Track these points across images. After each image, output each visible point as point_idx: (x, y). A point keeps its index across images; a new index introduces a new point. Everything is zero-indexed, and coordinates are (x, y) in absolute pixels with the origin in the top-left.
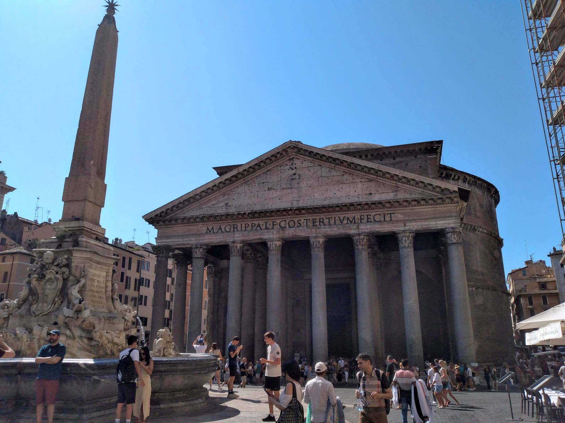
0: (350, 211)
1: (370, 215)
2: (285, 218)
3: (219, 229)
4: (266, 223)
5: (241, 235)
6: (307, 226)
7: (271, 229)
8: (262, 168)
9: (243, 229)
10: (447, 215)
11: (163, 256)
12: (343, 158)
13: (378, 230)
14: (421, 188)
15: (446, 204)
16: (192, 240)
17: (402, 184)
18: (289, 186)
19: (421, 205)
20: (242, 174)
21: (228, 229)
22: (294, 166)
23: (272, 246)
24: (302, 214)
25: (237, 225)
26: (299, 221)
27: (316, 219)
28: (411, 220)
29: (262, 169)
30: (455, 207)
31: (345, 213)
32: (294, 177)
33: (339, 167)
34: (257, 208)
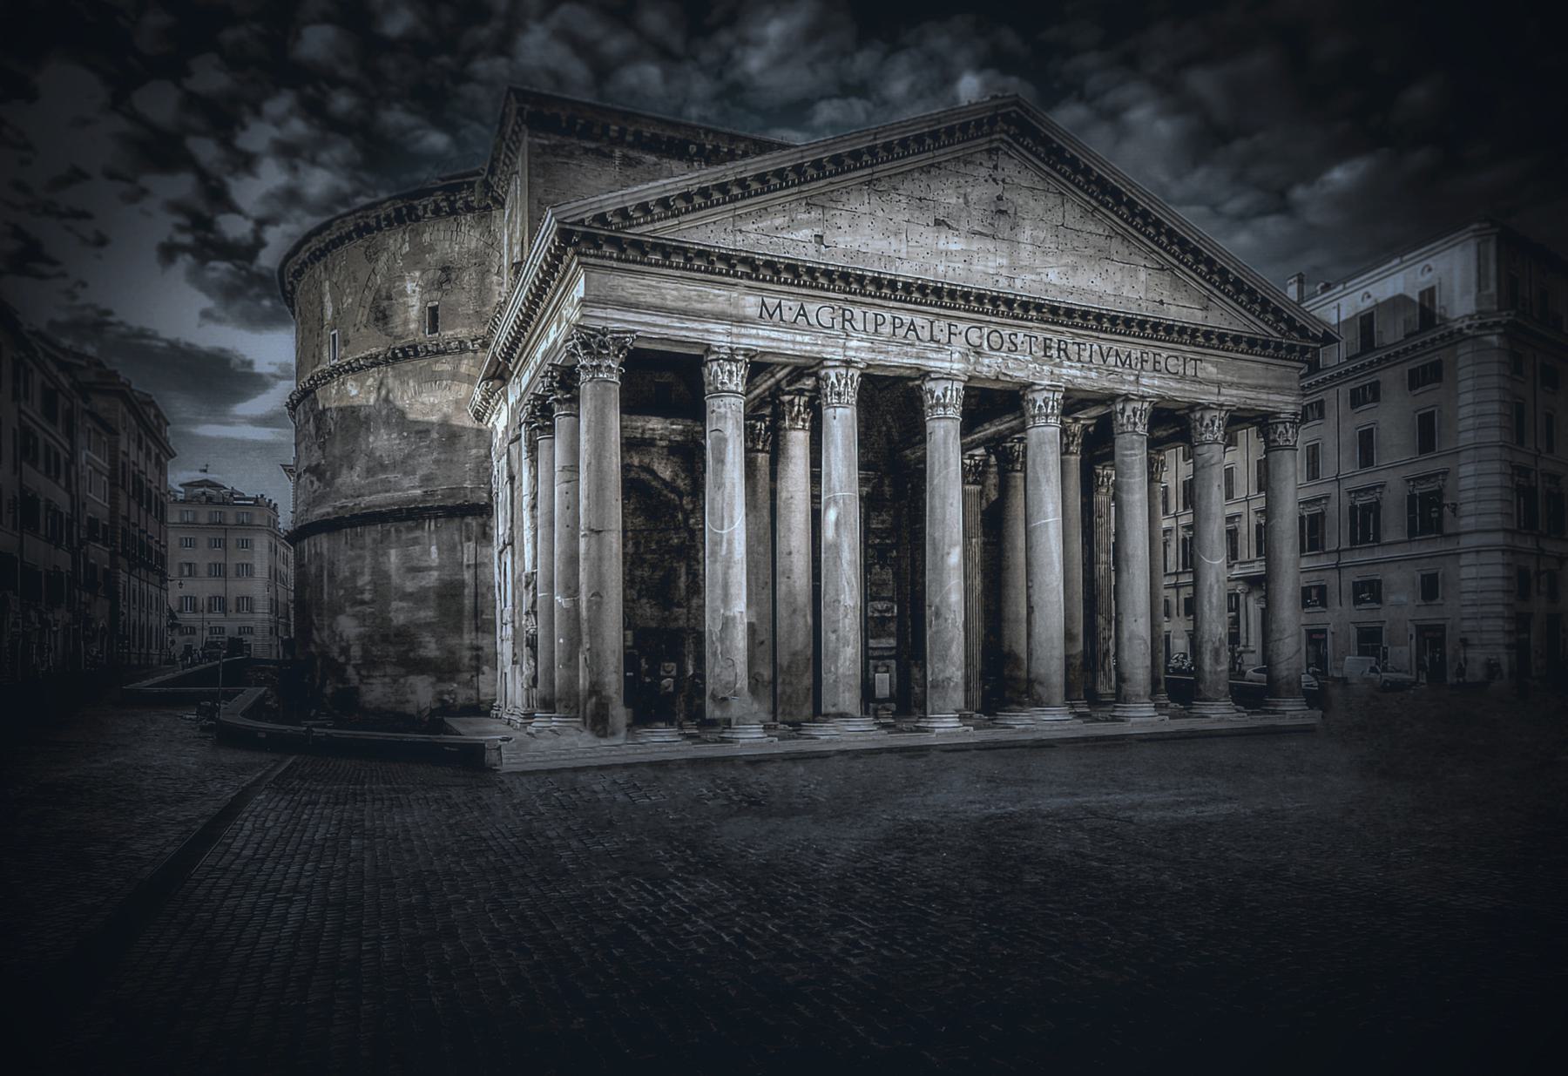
0: (1129, 335)
1: (1159, 355)
3: (799, 314)
4: (932, 323)
5: (869, 345)
6: (1031, 353)
9: (871, 328)
10: (1286, 384)
14: (1253, 314)
15: (1290, 360)
16: (714, 333)
21: (825, 318)
22: (999, 175)
23: (949, 392)
24: (1026, 320)
26: (1013, 337)
27: (1051, 340)
31: (1117, 337)
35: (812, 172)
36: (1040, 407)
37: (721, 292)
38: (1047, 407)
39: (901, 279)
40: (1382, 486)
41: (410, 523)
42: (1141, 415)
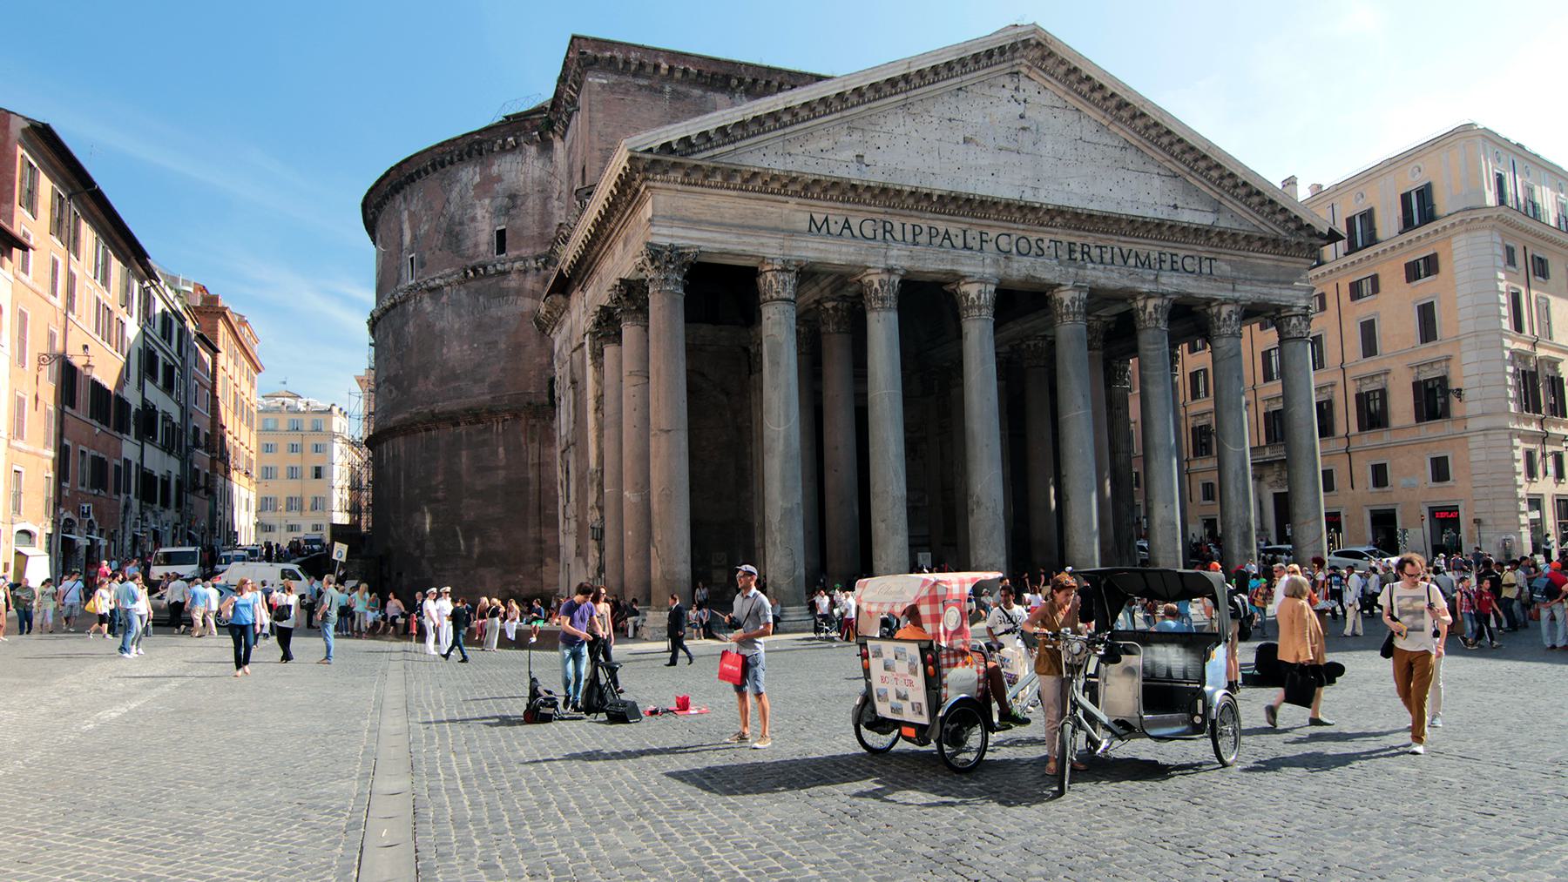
0: (1147, 237)
1: (1176, 255)
2: (1009, 229)
3: (844, 227)
4: (965, 232)
5: (908, 253)
8: (952, 77)
9: (909, 237)
13: (1190, 291)
14: (1262, 214)
18: (1013, 146)
19: (1262, 252)
22: (1021, 96)
23: (983, 296)
24: (1051, 226)
26: (1039, 242)
27: (1074, 244)
28: (1246, 279)
35: (855, 99)
36: (1067, 306)
38: (1074, 307)
40: (1387, 373)
41: (480, 426)
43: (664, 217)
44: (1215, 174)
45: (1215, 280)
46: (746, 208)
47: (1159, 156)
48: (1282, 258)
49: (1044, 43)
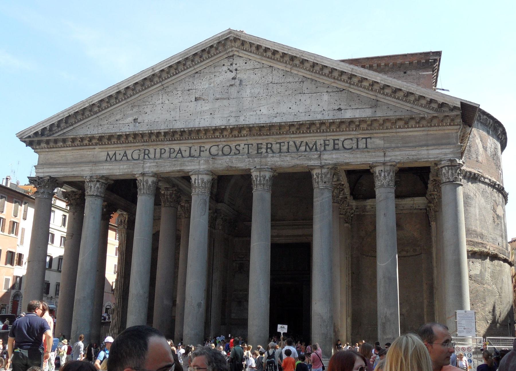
0: (310, 133)
1: (338, 140)
2: (216, 142)
3: (123, 156)
4: (190, 148)
5: (155, 164)
6: (248, 153)
7: (197, 158)
8: (188, 68)
9: (158, 155)
10: (444, 141)
11: (44, 192)
12: (304, 57)
13: (347, 161)
14: (409, 102)
16: (85, 171)
17: (384, 97)
19: (408, 127)
20: (160, 77)
21: (136, 156)
23: (197, 181)
24: (241, 136)
25: (149, 151)
26: (237, 147)
27: (262, 144)
28: (394, 148)
29: (189, 70)
30: (455, 131)
31: (303, 135)
32: (233, 82)
33: (299, 69)
34: (179, 125)
37: (91, 153)
39: (162, 131)
42: (322, 177)
43: (42, 164)
44: (365, 84)
45: (368, 152)
46: (78, 154)
47: (328, 81)
48: (427, 129)
49: (237, 37)
